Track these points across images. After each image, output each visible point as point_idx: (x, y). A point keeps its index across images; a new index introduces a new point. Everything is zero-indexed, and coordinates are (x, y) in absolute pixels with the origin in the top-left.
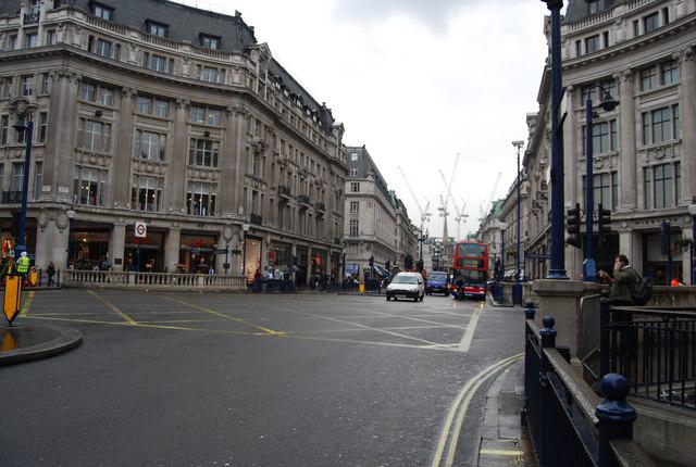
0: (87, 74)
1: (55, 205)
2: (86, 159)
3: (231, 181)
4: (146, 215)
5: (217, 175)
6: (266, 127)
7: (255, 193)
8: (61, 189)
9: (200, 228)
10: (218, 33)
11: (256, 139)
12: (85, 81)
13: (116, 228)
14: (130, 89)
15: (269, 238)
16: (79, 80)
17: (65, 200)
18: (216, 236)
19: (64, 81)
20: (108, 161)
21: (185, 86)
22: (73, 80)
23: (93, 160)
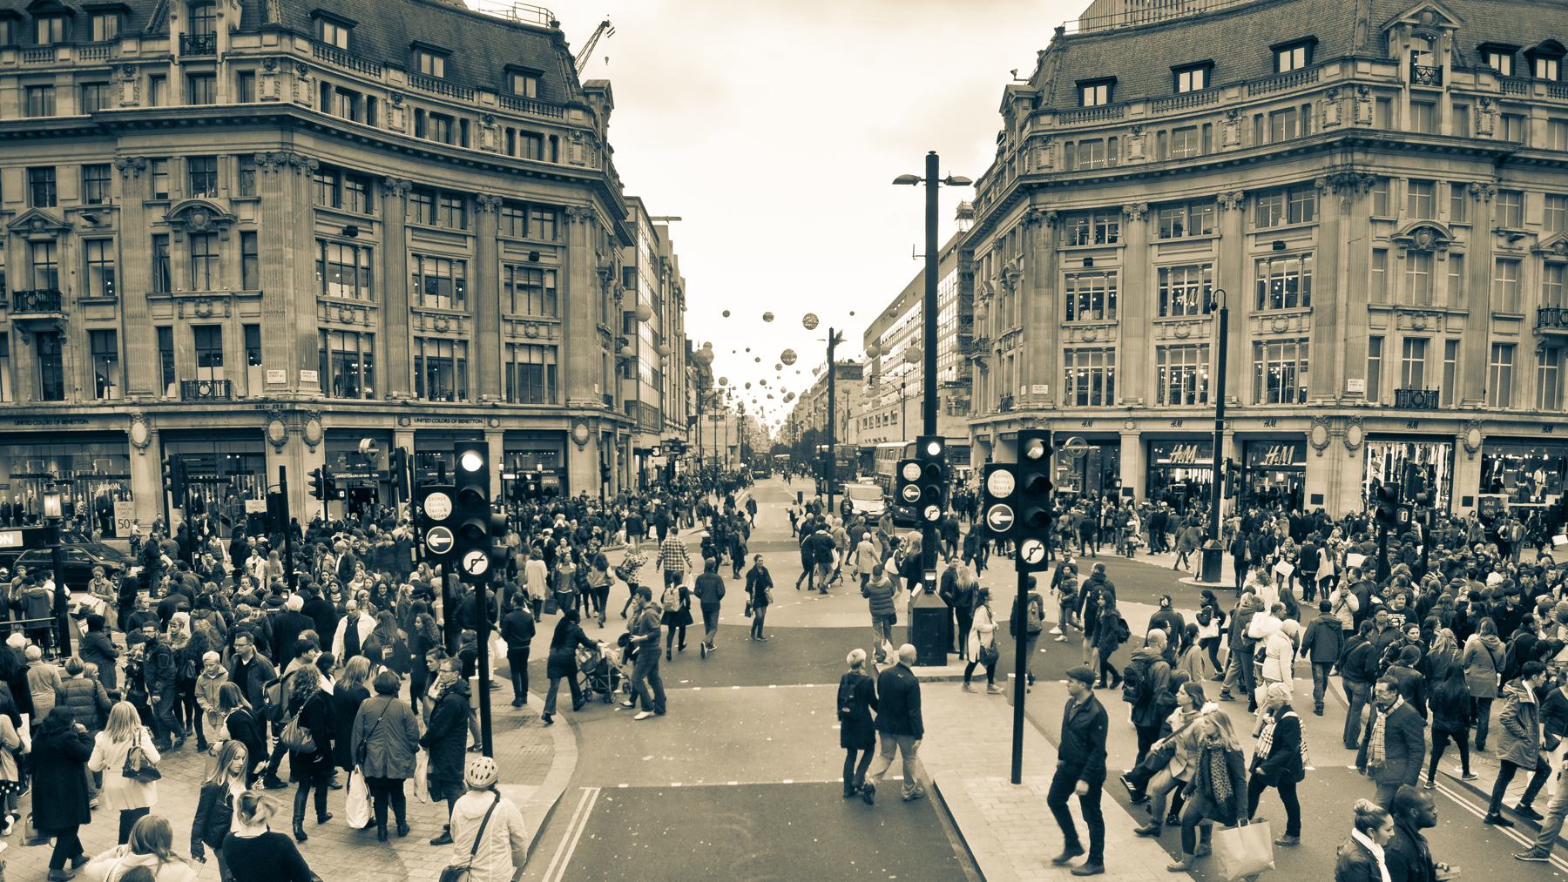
0: (1062, 207)
1: (1028, 415)
2: (1078, 336)
3: (1326, 329)
4: (1171, 414)
5: (1306, 321)
6: (1458, 187)
7: (1417, 344)
8: (1036, 389)
9: (1270, 429)
10: (1302, 33)
11: (1405, 223)
12: (1061, 217)
13: (1123, 440)
14: (1135, 206)
15: (1475, 437)
16: (1052, 220)
17: (1040, 406)
18: (1299, 443)
19: (1035, 226)
20: (1112, 333)
21: (1228, 166)
22: (1045, 226)
23: (1089, 335)
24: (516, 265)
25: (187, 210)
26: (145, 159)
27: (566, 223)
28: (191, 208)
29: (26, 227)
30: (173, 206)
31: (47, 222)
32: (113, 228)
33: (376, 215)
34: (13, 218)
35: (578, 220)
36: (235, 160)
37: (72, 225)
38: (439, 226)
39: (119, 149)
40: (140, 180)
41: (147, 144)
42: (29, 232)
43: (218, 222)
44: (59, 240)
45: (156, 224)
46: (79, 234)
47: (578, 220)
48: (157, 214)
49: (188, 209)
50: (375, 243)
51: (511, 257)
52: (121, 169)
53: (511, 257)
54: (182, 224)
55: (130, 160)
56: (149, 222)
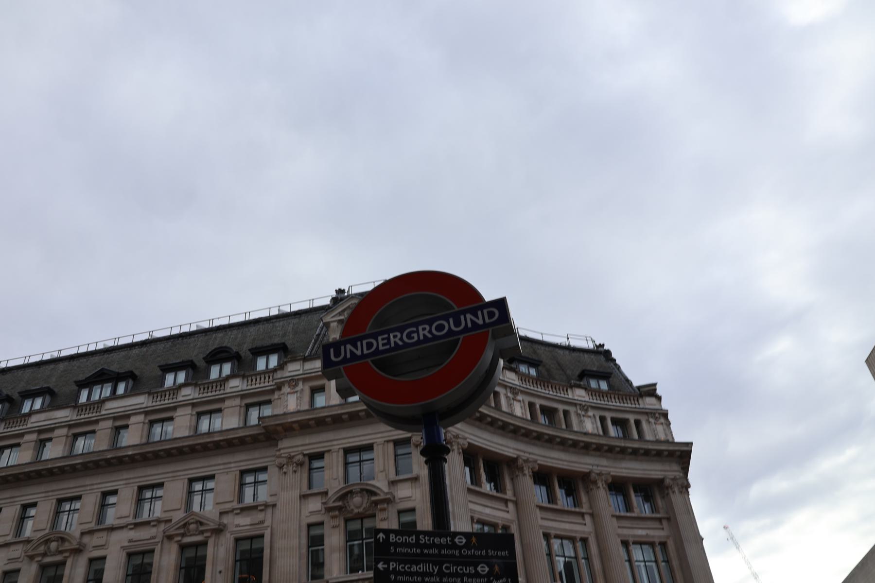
24: (631, 540)
25: (345, 496)
26: (304, 455)
27: (665, 496)
28: (351, 492)
29: (182, 531)
30: (330, 494)
31: (201, 524)
32: (266, 524)
33: (509, 495)
34: (168, 525)
35: (676, 489)
36: (391, 445)
37: (225, 526)
38: (560, 505)
39: (280, 450)
40: (298, 474)
41: (307, 442)
42: (183, 535)
43: (376, 503)
44: (211, 543)
45: (312, 513)
46: (232, 533)
47: (676, 489)
48: (315, 505)
49: (346, 494)
50: (512, 522)
51: (625, 532)
52: (281, 467)
53: (625, 532)
54: (340, 509)
55: (290, 458)
56: (305, 512)
